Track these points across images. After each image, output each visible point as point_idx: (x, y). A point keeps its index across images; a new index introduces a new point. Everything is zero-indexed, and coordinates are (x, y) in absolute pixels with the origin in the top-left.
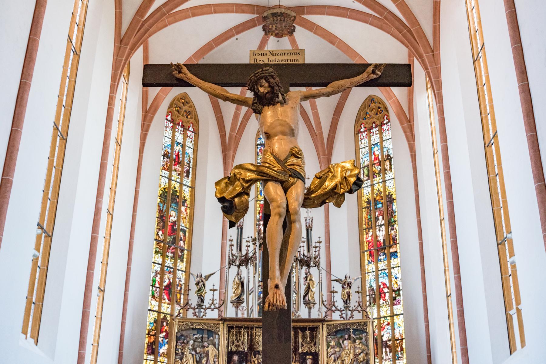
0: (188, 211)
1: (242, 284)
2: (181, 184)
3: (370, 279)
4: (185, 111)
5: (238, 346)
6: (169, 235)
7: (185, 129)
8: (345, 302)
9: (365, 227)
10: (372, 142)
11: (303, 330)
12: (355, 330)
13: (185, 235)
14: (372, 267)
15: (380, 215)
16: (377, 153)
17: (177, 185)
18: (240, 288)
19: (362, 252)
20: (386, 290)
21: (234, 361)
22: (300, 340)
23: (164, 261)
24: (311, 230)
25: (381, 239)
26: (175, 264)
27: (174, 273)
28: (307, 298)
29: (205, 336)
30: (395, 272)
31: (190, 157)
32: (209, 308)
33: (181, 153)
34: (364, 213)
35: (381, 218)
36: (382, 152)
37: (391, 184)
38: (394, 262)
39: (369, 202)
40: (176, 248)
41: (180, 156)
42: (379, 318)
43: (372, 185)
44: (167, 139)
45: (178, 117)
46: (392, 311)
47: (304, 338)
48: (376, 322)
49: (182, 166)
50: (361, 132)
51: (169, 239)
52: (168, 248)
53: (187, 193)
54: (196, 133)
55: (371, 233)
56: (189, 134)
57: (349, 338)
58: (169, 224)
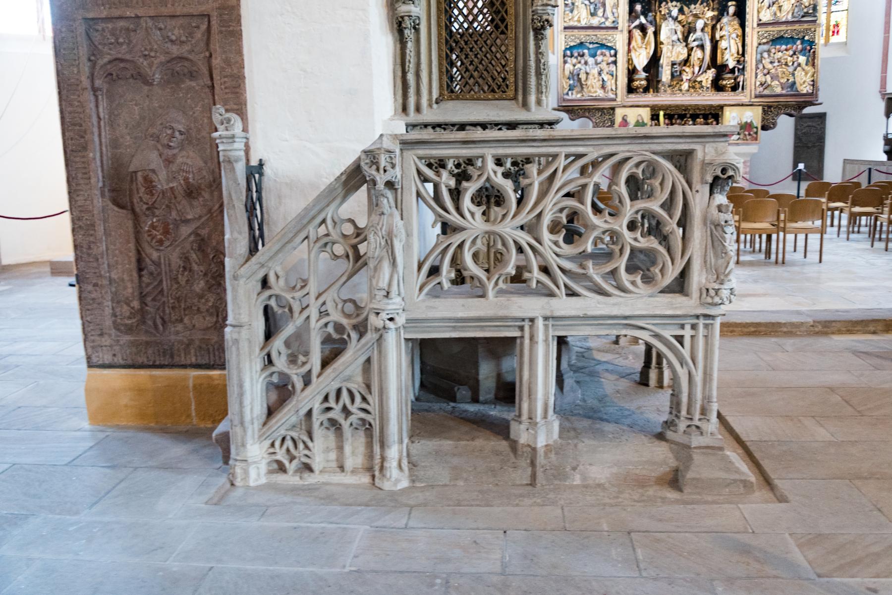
21: (636, 12)
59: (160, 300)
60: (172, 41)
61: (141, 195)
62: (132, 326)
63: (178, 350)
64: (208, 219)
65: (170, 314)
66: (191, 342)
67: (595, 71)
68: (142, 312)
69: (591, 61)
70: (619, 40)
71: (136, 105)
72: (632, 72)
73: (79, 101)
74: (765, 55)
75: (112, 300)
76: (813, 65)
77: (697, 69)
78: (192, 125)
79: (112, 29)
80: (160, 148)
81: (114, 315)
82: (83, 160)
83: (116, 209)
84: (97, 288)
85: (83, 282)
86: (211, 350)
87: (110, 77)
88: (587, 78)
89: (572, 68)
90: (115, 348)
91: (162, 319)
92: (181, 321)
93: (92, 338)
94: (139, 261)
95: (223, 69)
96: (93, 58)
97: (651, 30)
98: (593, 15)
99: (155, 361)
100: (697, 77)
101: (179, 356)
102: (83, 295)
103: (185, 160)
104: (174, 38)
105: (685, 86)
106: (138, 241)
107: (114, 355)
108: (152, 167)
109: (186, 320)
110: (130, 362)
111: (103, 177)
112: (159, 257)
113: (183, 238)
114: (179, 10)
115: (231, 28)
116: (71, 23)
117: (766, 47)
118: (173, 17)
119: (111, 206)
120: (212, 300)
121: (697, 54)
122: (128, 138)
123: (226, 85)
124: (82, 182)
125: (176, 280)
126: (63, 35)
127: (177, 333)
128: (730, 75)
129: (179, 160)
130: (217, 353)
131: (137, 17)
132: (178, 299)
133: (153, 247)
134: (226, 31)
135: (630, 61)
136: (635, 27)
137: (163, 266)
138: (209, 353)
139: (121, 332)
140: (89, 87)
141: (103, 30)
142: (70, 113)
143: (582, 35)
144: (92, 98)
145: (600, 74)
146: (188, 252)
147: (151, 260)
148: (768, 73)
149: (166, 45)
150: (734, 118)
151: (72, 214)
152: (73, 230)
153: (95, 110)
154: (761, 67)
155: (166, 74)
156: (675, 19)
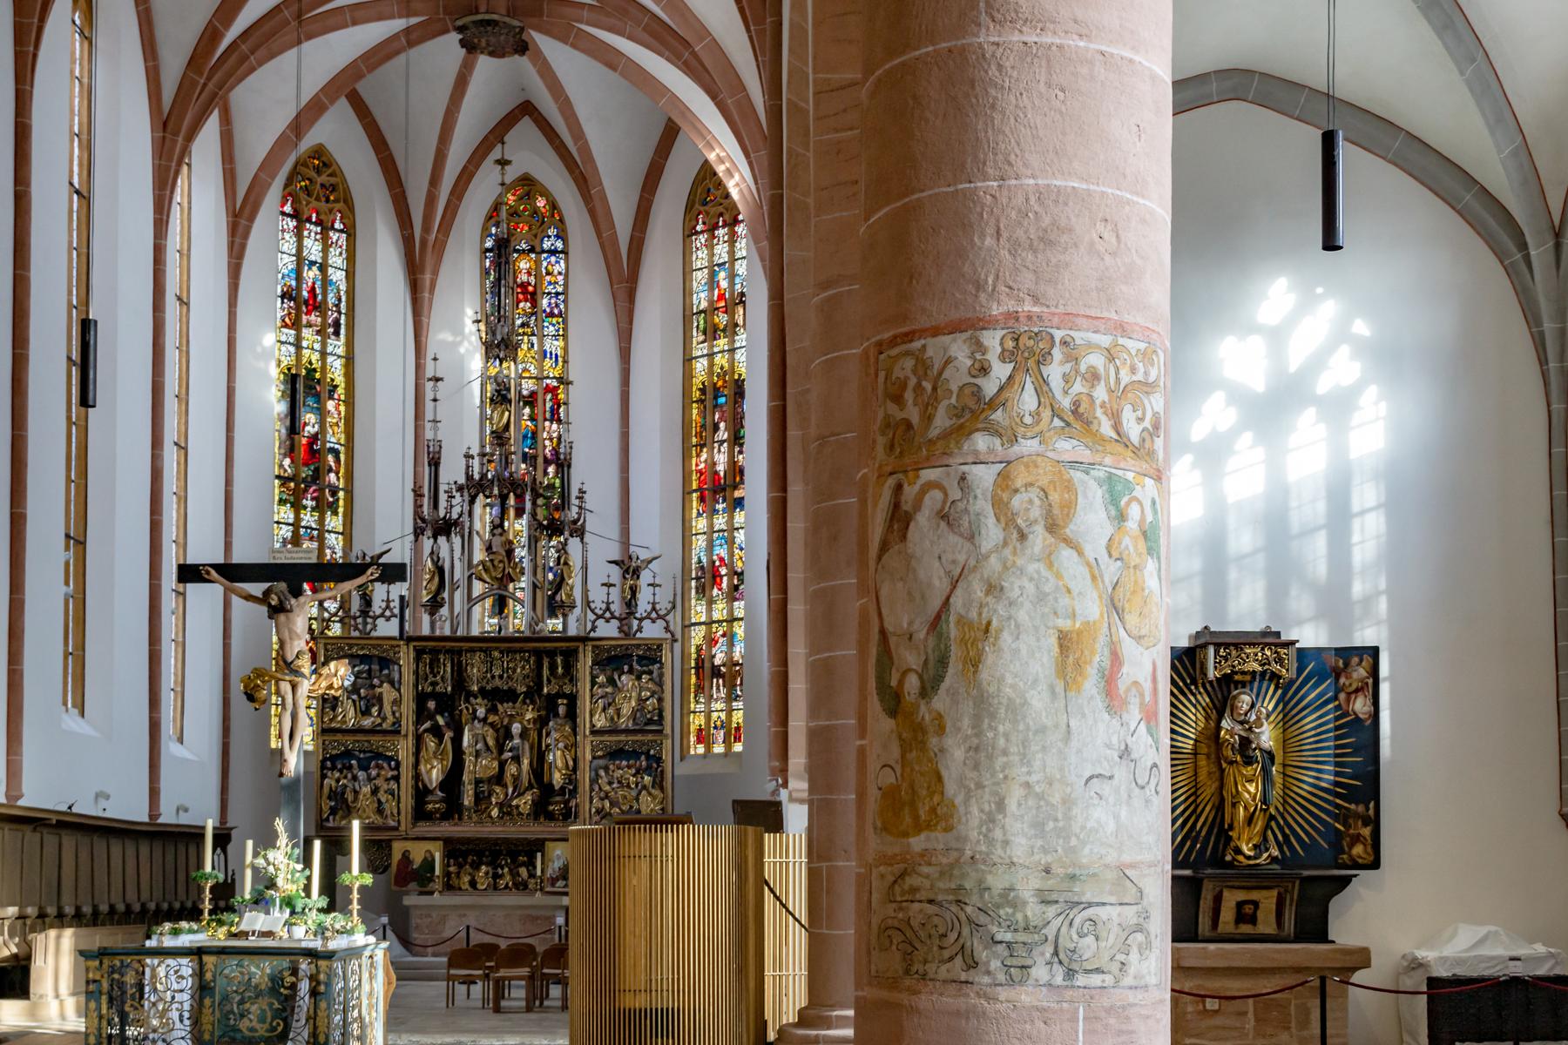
0: (342, 408)
1: (441, 570)
2: (324, 354)
3: (700, 543)
4: (323, 185)
5: (434, 684)
6: (306, 464)
7: (325, 228)
8: (629, 604)
9: (694, 440)
10: (716, 260)
11: (552, 654)
12: (641, 659)
13: (338, 460)
14: (701, 524)
15: (721, 419)
16: (724, 284)
17: (315, 357)
18: (437, 579)
19: (686, 493)
20: (723, 571)
22: (546, 672)
23: (298, 518)
24: (569, 466)
25: (721, 468)
26: (321, 521)
27: (321, 539)
28: (558, 598)
29: (375, 667)
30: (740, 537)
31: (339, 291)
32: (382, 615)
33: (318, 283)
34: (695, 412)
35: (722, 425)
36: (732, 284)
37: (743, 359)
38: (739, 517)
39: (703, 391)
40: (321, 490)
41: (318, 291)
42: (709, 623)
43: (711, 356)
44: (286, 259)
45: (308, 203)
46: (731, 611)
47: (553, 668)
48: (702, 630)
49: (324, 316)
50: (697, 233)
51: (306, 472)
52: (306, 491)
53: (336, 370)
54: (350, 231)
55: (704, 456)
56: (334, 236)
57: (631, 671)
58: (304, 441)
67: (366, 789)
69: (361, 775)
70: (403, 749)
72: (421, 793)
74: (602, 773)
76: (662, 789)
77: (510, 790)
88: (356, 799)
89: (334, 784)
97: (448, 735)
98: (366, 713)
100: (512, 799)
105: (495, 813)
117: (602, 762)
121: (512, 769)
128: (558, 798)
135: (417, 777)
136: (426, 731)
143: (349, 741)
145: (375, 791)
148: (607, 797)
150: (559, 857)
154: (596, 788)
156: (484, 720)
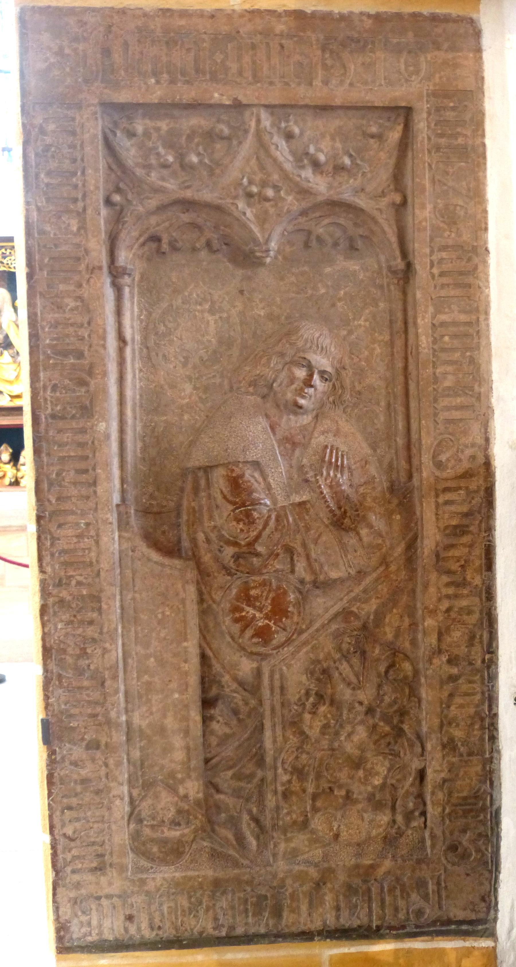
59: (252, 776)
60: (316, 165)
61: (219, 522)
62: (180, 842)
63: (293, 896)
64: (377, 580)
65: (278, 808)
66: (326, 875)
68: (209, 808)
71: (212, 311)
73: (80, 298)
75: (131, 783)
78: (347, 361)
79: (171, 132)
80: (273, 411)
81: (134, 815)
82: (80, 438)
83: (155, 556)
84: (98, 754)
85: (60, 739)
86: (374, 890)
87: (154, 245)
90: (133, 900)
91: (257, 821)
92: (304, 825)
93: (76, 877)
94: (207, 680)
95: (436, 230)
96: (117, 198)
99: (232, 928)
101: (295, 910)
102: (58, 773)
103: (331, 439)
104: (322, 158)
106: (204, 631)
107: (130, 918)
108: (251, 456)
109: (317, 823)
110: (168, 932)
111: (123, 481)
112: (258, 673)
113: (317, 625)
114: (340, 94)
115: (460, 140)
116: (70, 113)
118: (324, 109)
119: (143, 548)
120: (383, 770)
122: (188, 388)
123: (446, 267)
124: (74, 491)
125: (295, 724)
126: (48, 140)
127: (294, 853)
129: (318, 440)
130: (388, 899)
131: (238, 106)
132: (299, 772)
133: (242, 648)
134: (449, 147)
137: (266, 693)
138: (370, 899)
139: (150, 858)
140: (104, 261)
141: (147, 134)
142: (56, 325)
144: (109, 293)
146: (328, 656)
147: (235, 679)
149: (303, 174)
151: (42, 570)
152: (43, 610)
153: (118, 318)
155: (290, 243)
